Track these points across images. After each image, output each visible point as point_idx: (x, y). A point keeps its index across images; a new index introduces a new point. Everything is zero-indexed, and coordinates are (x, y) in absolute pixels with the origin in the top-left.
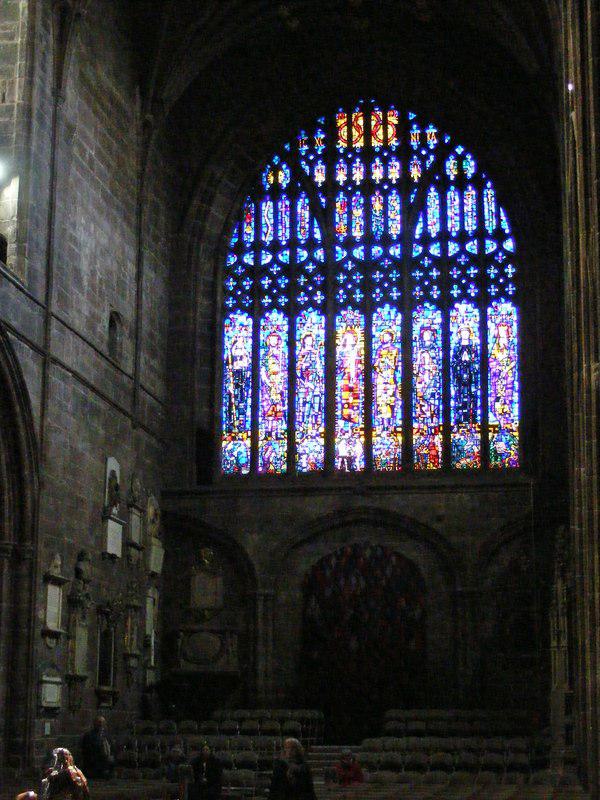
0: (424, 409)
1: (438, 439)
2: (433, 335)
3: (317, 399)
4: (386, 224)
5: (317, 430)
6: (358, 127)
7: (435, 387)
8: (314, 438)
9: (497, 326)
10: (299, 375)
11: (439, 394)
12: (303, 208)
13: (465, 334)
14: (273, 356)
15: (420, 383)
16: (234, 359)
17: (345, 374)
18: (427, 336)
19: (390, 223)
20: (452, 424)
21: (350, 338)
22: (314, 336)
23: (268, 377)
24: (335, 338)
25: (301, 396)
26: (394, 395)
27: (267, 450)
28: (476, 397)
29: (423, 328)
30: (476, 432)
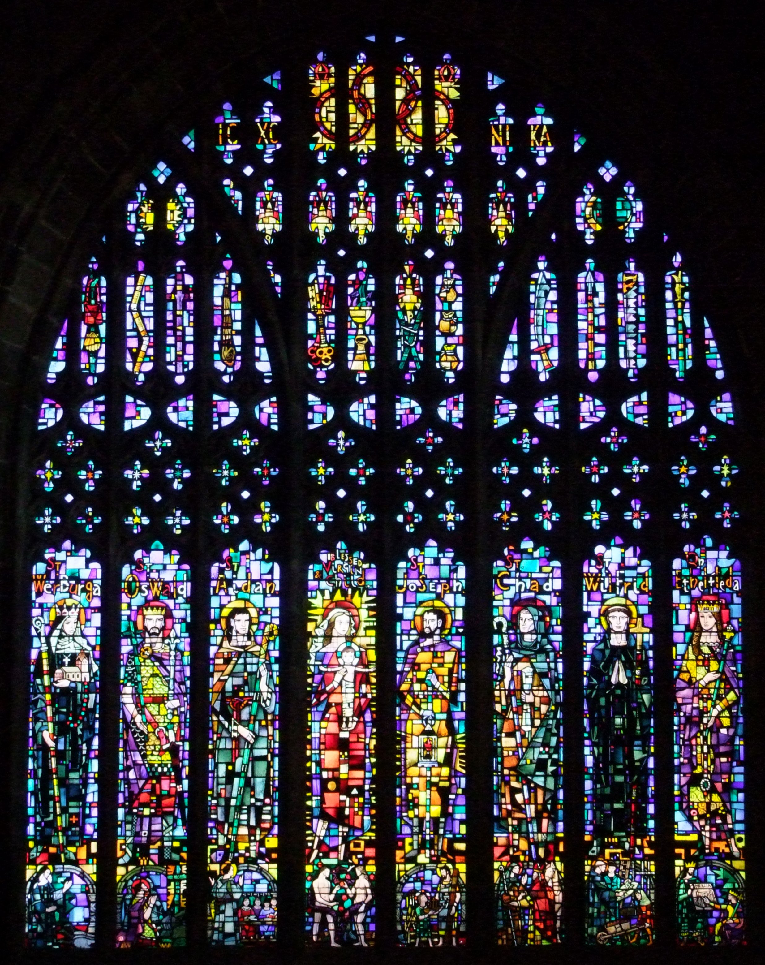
2: (541, 618)
3: (261, 767)
5: (262, 843)
8: (254, 861)
10: (217, 706)
15: (511, 735)
17: (329, 706)
22: (253, 613)
23: (141, 709)
24: (305, 619)
25: (222, 758)
26: (448, 761)
27: (137, 888)
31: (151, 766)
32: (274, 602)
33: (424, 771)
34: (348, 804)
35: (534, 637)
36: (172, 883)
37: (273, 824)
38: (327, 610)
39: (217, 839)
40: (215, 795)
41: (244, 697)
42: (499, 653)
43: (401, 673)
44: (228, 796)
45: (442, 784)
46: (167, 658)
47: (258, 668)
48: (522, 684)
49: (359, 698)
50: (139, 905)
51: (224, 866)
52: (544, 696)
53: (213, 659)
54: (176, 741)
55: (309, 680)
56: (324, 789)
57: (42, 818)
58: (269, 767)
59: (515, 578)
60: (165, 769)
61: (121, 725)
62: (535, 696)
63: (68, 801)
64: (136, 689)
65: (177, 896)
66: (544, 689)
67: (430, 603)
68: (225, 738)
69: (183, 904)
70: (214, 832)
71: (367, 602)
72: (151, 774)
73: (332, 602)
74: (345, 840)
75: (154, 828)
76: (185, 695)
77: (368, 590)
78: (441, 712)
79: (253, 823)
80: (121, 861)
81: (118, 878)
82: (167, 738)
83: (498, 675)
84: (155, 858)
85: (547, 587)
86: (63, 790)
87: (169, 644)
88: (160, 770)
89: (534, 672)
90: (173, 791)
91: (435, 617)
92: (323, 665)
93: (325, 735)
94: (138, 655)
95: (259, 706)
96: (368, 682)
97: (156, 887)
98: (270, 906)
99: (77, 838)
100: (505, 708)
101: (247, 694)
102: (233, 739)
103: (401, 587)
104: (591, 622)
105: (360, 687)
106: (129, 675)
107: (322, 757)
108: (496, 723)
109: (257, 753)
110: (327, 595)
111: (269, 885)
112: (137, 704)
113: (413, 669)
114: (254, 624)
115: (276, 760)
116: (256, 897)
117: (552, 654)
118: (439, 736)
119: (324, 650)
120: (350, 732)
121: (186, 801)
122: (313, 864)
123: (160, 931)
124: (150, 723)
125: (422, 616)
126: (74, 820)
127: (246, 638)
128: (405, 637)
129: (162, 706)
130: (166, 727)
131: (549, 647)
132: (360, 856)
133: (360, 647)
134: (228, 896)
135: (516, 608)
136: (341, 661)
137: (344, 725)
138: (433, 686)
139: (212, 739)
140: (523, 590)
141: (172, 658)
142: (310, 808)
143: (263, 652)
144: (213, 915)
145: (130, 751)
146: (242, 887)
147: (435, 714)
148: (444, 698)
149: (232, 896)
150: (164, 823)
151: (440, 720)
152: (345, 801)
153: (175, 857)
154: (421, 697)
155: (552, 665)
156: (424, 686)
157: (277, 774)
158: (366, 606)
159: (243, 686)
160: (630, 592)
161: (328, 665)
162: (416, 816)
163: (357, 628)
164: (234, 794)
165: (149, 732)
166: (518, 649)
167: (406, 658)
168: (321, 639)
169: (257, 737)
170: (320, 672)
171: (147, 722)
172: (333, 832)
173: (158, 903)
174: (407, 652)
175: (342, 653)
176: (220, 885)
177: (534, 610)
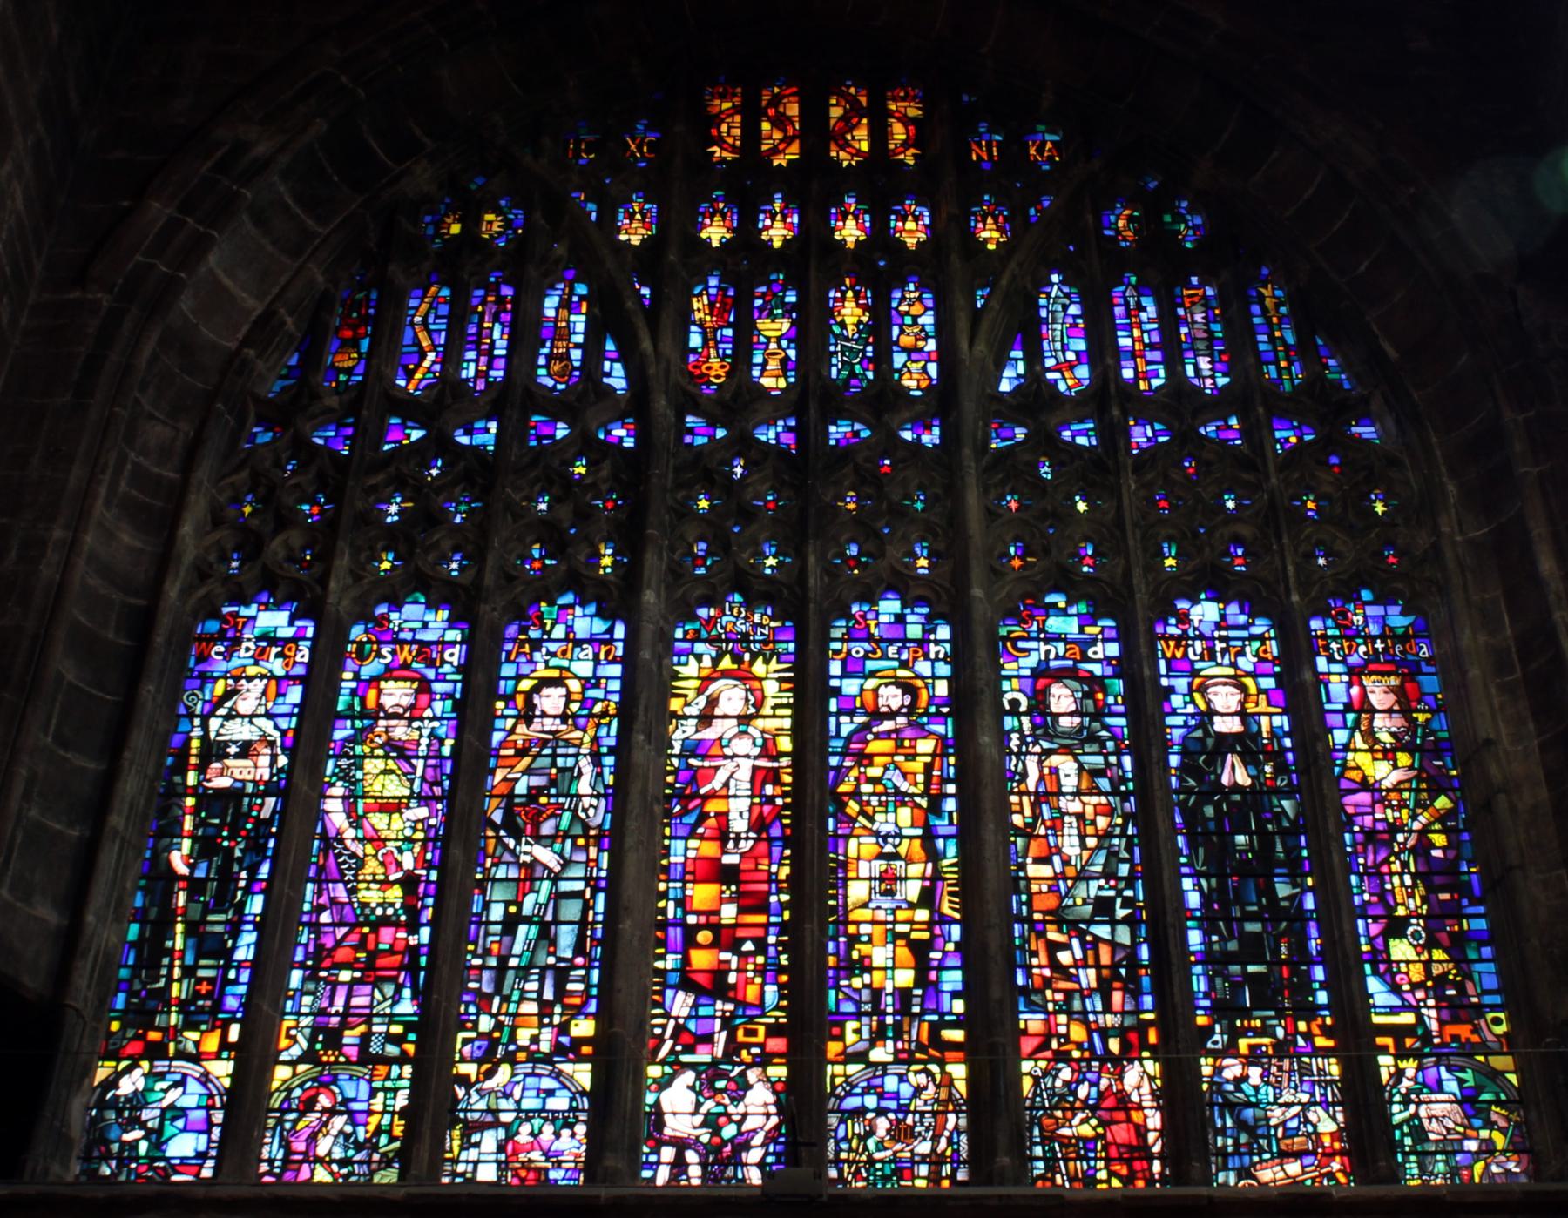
0: (1064, 957)
1: (1140, 1078)
2: (1086, 695)
3: (571, 910)
4: (882, 359)
5: (563, 1029)
6: (780, 122)
7: (1109, 874)
8: (547, 1059)
9: (1355, 673)
10: (497, 817)
11: (1127, 903)
12: (566, 305)
13: (1225, 699)
16: (214, 751)
17: (703, 817)
18: (1062, 698)
19: (899, 359)
20: (1202, 1020)
21: (732, 698)
22: (575, 686)
23: (356, 820)
24: (668, 693)
25: (499, 893)
26: (928, 898)
27: (308, 1105)
28: (1301, 916)
29: (1044, 674)
30: (1317, 1052)
31: (364, 905)
32: (616, 670)
33: (881, 915)
34: (734, 965)
35: (1077, 720)
36: (381, 1095)
37: (590, 997)
38: (706, 681)
39: (476, 1023)
41: (549, 804)
43: (838, 768)
44: (503, 952)
45: (914, 935)
48: (1059, 785)
49: (761, 804)
50: (309, 1131)
51: (485, 1067)
53: (497, 750)
55: (670, 779)
56: (690, 941)
57: (144, 985)
58: (586, 908)
59: (1038, 639)
61: (316, 843)
62: (1084, 804)
63: (198, 957)
66: (1100, 793)
67: (890, 673)
68: (508, 864)
69: (398, 1131)
70: (472, 1009)
74: (728, 1023)
75: (355, 1001)
76: (438, 799)
77: (779, 655)
78: (913, 826)
79: (548, 995)
80: (284, 1057)
81: (275, 1085)
82: (399, 865)
83: (1015, 772)
84: (353, 1052)
86: (191, 942)
87: (419, 729)
89: (1081, 768)
90: (400, 946)
91: (899, 691)
92: (695, 756)
93: (695, 859)
94: (362, 743)
95: (575, 817)
96: (777, 781)
97: (346, 1101)
98: (573, 1135)
99: (206, 1018)
101: (553, 800)
102: (521, 866)
103: (837, 652)
104: (1176, 701)
105: (762, 788)
107: (688, 892)
108: (1015, 843)
109: (565, 886)
110: (707, 662)
111: (573, 1099)
112: (350, 811)
113: (859, 764)
115: (601, 897)
116: (546, 1119)
117: (1110, 745)
118: (909, 860)
119: (699, 736)
120: (742, 855)
121: (423, 961)
122: (663, 1063)
124: (371, 840)
125: (875, 691)
126: (204, 988)
127: (558, 721)
128: (844, 719)
129: (396, 816)
131: (1104, 733)
133: (763, 732)
134: (489, 1118)
135: (1042, 683)
136: (727, 751)
137: (731, 845)
138: (895, 787)
139: (483, 865)
140: (1052, 656)
143: (587, 739)
144: (456, 1149)
145: (328, 882)
146: (518, 1103)
148: (917, 806)
149: (497, 1119)
150: (377, 994)
151: (911, 838)
152: (728, 962)
153: (392, 1050)
155: (1113, 759)
156: (880, 788)
157: (600, 918)
159: (547, 788)
160: (1241, 661)
161: (705, 757)
162: (865, 986)
163: (759, 705)
164: (517, 949)
166: (1049, 737)
167: (846, 746)
168: (694, 721)
169: (566, 863)
170: (690, 767)
172: (702, 1011)
173: (349, 1129)
174: (849, 739)
176: (475, 1097)
177: (1075, 685)
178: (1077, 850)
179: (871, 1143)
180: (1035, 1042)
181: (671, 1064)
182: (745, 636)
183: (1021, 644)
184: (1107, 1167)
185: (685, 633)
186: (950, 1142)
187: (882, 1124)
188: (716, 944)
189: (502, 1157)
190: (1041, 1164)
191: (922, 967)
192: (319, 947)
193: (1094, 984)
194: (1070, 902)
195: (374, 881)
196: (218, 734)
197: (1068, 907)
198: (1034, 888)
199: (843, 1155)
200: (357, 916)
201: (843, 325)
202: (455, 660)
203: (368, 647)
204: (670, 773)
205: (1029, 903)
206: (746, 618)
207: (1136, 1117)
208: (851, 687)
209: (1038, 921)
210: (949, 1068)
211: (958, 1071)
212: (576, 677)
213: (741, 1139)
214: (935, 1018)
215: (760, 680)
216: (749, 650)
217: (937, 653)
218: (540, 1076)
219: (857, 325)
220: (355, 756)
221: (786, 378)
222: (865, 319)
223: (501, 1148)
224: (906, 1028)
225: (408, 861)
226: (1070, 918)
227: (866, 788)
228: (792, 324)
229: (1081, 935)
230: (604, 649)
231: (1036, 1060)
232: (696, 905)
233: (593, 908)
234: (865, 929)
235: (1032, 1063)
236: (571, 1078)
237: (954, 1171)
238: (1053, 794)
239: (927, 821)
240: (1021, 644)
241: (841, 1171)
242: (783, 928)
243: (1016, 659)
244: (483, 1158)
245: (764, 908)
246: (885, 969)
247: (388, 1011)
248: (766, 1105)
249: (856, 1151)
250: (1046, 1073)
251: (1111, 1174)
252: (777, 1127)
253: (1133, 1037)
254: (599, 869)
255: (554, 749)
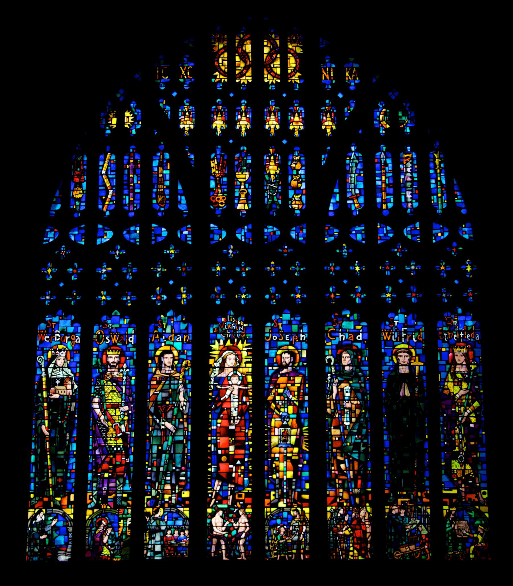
0: (343, 466)
2: (356, 357)
3: (179, 448)
4: (284, 195)
7: (359, 433)
8: (174, 506)
10: (152, 410)
11: (365, 445)
14: (113, 380)
16: (51, 382)
17: (222, 410)
18: (346, 359)
19: (291, 193)
22: (176, 353)
23: (104, 412)
25: (155, 442)
26: (298, 443)
34: (234, 470)
35: (351, 368)
36: (122, 521)
38: (222, 351)
39: (151, 492)
40: (150, 465)
41: (169, 404)
42: (329, 378)
45: (293, 458)
46: (121, 380)
47: (178, 387)
48: (344, 396)
49: (242, 404)
51: (155, 509)
52: (357, 404)
54: (126, 431)
58: (184, 447)
60: (119, 449)
62: (352, 404)
64: (101, 399)
65: (125, 528)
67: (286, 347)
70: (149, 488)
71: (246, 347)
72: (109, 452)
73: (225, 347)
77: (247, 339)
78: (293, 414)
79: (174, 482)
80: (89, 506)
81: (87, 517)
82: (120, 430)
83: (329, 391)
85: (359, 338)
87: (122, 372)
88: (115, 449)
89: (351, 389)
90: (123, 463)
91: (289, 356)
92: (218, 385)
93: (220, 427)
94: (103, 379)
95: (179, 410)
96: (247, 395)
98: (184, 534)
100: (333, 411)
103: (268, 338)
105: (242, 398)
106: (97, 391)
107: (218, 441)
109: (177, 438)
110: (222, 342)
111: (183, 521)
112: (101, 407)
113: (275, 387)
114: (176, 360)
115: (189, 443)
116: (175, 529)
117: (362, 378)
118: (292, 428)
119: (220, 375)
122: (212, 508)
123: (113, 550)
125: (281, 355)
126: (60, 480)
127: (171, 369)
128: (270, 368)
129: (117, 410)
130: (119, 423)
131: (360, 374)
132: (241, 503)
133: (242, 374)
134: (157, 529)
135: (339, 351)
136: (230, 382)
137: (232, 422)
140: (344, 339)
141: (124, 380)
142: (210, 473)
143: (181, 377)
144: (148, 540)
146: (166, 523)
147: (289, 414)
148: (295, 405)
149: (160, 528)
150: (117, 482)
151: (293, 418)
152: (232, 468)
153: (124, 503)
154: (280, 404)
155: (363, 385)
156: (282, 397)
158: (246, 349)
159: (168, 397)
162: (277, 478)
163: (240, 362)
164: (162, 464)
165: (109, 426)
167: (270, 380)
168: (217, 369)
171: (107, 420)
173: (113, 533)
174: (272, 377)
175: (231, 377)
176: (152, 521)
177: (351, 352)
178: (348, 423)
179: (279, 537)
180: (332, 499)
181: (215, 508)
182: (235, 330)
183: (333, 334)
184: (353, 546)
185: (214, 330)
186: (304, 537)
187: (282, 530)
188: (229, 462)
189: (162, 542)
190: (332, 545)
191: (296, 470)
192: (97, 463)
193: (352, 477)
194: (346, 444)
195: (112, 437)
196: (52, 375)
197: (345, 446)
198: (334, 439)
199: (270, 541)
200: (108, 451)
201: (269, 175)
202: (132, 341)
203: (101, 336)
204: (210, 391)
205: (332, 445)
206: (235, 322)
207: (363, 528)
208: (272, 353)
209: (334, 452)
210: (304, 509)
211: (307, 510)
212: (176, 350)
213: (237, 536)
214: (300, 490)
215: (241, 351)
216: (236, 337)
217: (303, 338)
218: (173, 512)
219: (275, 175)
220: (101, 385)
221: (248, 204)
222: (278, 172)
223: (162, 538)
224: (290, 494)
225: (123, 430)
226: (345, 451)
227: (278, 398)
228: (250, 175)
229: (348, 457)
230: (185, 337)
231: (332, 506)
232: (221, 446)
233: (187, 447)
234: (277, 455)
235: (330, 507)
236: (183, 513)
237: (305, 547)
238: (341, 400)
239: (298, 411)
240: (333, 334)
241: (269, 547)
242: (250, 455)
243: (331, 341)
244: (156, 543)
245: (243, 447)
246: (284, 471)
247: (122, 488)
248: (245, 523)
249: (274, 540)
250: (335, 511)
251: (354, 548)
252: (249, 531)
253: (364, 497)
254: (188, 432)
255: (170, 382)
